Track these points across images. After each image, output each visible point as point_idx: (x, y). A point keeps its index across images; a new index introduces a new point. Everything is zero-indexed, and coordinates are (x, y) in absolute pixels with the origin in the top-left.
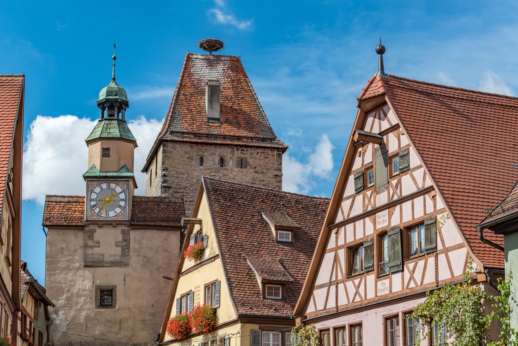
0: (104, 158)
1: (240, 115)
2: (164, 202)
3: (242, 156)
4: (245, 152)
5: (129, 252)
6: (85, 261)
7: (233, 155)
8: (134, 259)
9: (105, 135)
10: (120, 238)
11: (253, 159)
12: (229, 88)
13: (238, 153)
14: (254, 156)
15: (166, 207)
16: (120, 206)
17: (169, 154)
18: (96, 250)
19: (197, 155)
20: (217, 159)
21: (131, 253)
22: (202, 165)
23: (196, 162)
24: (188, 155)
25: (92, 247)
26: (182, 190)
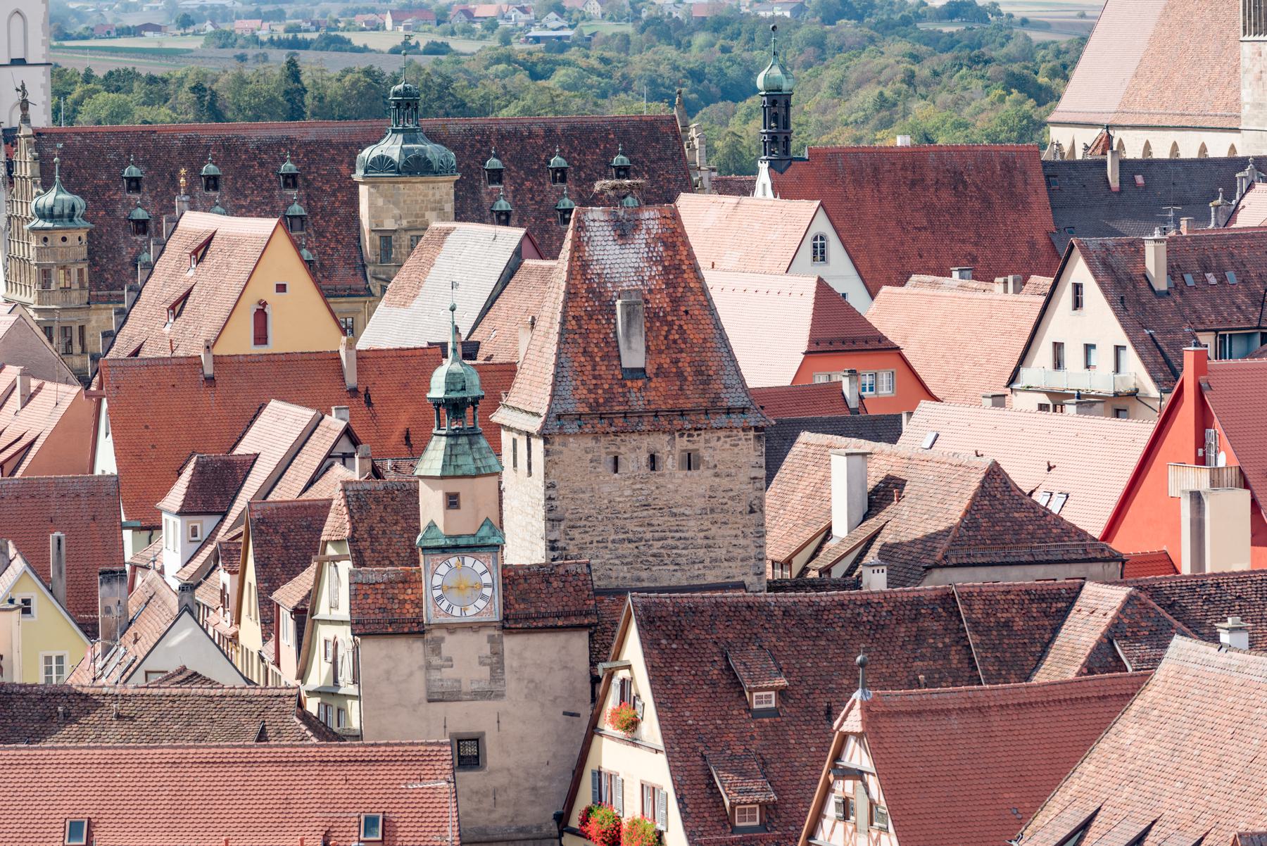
0: (451, 511)
1: (684, 355)
2: (556, 575)
3: (690, 446)
4: (695, 438)
5: (503, 673)
6: (429, 693)
7: (673, 446)
8: (511, 685)
9: (451, 471)
10: (487, 650)
11: (711, 451)
12: (661, 290)
13: (682, 443)
14: (712, 445)
15: (561, 585)
16: (483, 597)
17: (555, 458)
18: (447, 673)
19: (608, 454)
20: (644, 458)
21: (507, 675)
22: (616, 471)
23: (605, 468)
24: (590, 456)
25: (439, 668)
26: (582, 523)
